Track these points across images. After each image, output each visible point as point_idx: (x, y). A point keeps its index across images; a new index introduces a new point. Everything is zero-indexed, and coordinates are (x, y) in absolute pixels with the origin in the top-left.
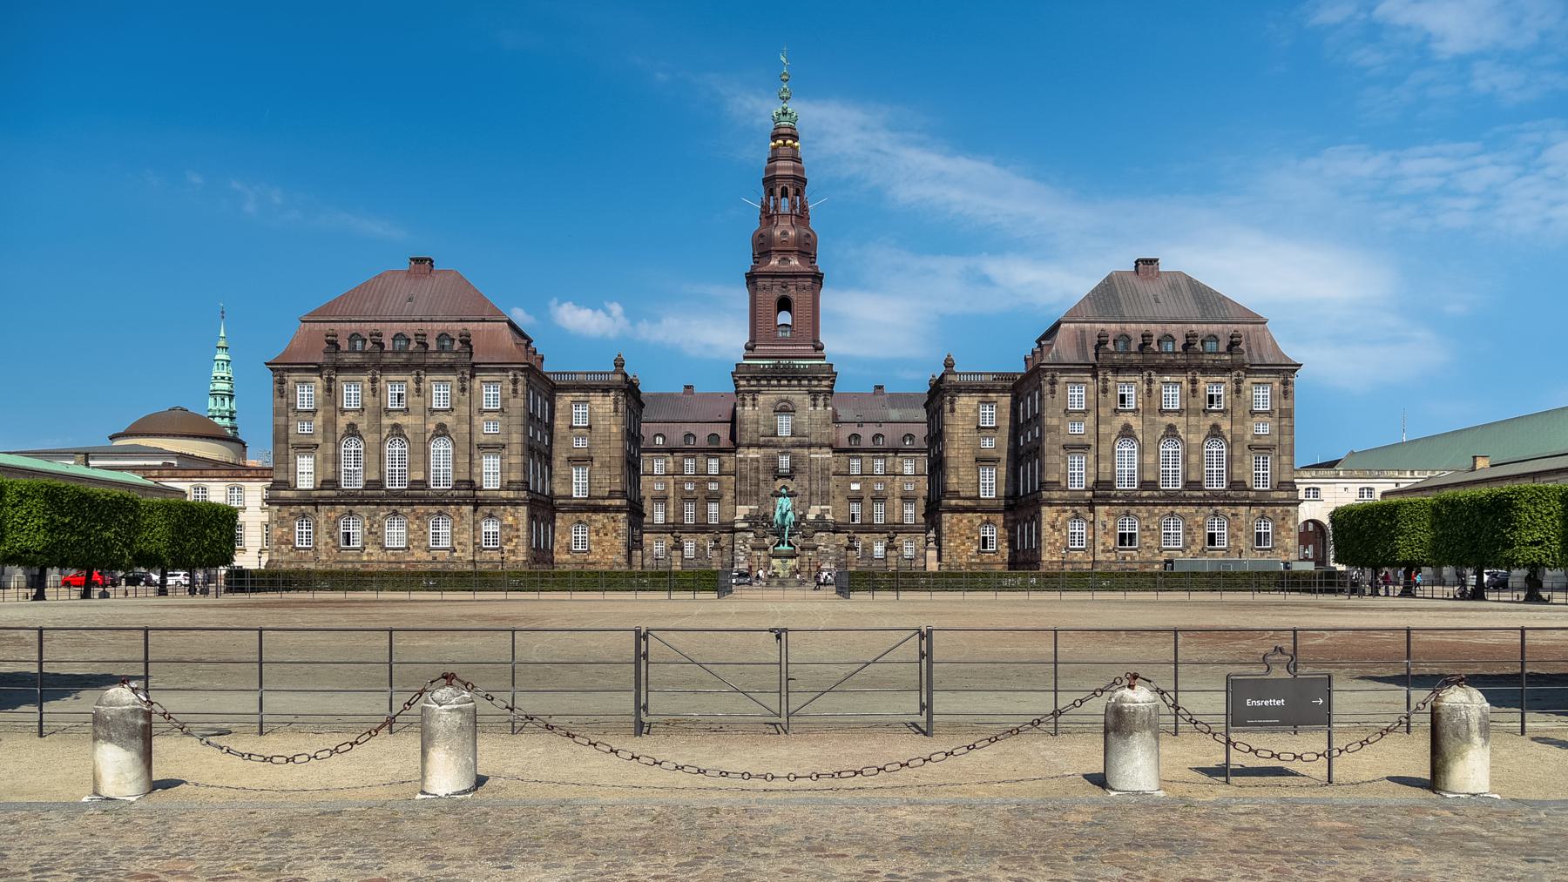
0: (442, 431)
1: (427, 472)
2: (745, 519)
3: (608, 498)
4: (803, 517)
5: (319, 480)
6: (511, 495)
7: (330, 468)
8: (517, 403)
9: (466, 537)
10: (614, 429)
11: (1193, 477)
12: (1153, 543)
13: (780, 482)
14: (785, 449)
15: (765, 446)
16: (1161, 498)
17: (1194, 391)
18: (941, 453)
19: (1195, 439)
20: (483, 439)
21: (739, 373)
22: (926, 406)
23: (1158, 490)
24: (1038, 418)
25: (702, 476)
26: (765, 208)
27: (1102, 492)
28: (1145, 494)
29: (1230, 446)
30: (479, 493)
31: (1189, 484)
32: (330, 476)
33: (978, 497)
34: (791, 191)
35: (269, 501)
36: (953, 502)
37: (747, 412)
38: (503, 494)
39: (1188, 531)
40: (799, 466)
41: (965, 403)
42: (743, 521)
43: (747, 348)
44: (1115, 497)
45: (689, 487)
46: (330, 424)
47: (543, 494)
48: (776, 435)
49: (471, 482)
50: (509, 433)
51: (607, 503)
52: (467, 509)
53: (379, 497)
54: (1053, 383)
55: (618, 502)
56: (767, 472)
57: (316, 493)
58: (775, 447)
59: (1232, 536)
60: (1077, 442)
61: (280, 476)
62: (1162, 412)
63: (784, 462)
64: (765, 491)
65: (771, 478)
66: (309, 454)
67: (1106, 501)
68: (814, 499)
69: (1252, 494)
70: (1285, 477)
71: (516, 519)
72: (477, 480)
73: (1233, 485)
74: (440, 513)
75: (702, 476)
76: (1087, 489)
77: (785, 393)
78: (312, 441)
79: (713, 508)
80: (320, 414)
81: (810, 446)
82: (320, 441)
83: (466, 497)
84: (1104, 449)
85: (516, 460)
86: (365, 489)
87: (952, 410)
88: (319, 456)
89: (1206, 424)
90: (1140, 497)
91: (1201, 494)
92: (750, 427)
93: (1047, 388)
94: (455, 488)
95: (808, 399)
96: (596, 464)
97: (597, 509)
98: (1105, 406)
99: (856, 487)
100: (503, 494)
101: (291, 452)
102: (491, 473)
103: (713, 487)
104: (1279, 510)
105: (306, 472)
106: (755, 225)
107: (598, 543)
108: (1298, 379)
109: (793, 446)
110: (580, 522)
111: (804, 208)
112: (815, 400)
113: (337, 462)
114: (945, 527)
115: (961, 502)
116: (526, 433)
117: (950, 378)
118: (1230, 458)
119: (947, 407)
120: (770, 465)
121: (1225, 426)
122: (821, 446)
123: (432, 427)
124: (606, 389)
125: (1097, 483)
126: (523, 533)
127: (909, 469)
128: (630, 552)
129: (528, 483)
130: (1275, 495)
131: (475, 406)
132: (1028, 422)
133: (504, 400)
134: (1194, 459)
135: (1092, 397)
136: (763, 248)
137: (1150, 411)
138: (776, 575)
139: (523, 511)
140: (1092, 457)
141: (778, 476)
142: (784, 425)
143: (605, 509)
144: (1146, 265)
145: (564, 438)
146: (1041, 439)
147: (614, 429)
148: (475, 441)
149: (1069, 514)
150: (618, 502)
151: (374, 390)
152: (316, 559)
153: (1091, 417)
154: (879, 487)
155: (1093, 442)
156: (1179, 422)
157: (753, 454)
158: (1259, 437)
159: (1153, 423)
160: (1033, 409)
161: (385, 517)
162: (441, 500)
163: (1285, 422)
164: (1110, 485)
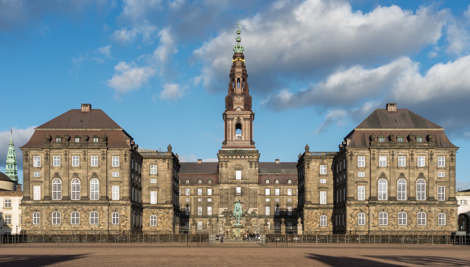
0: (95, 175)
1: (88, 193)
2: (223, 213)
3: (166, 204)
4: (246, 212)
5: (43, 196)
6: (124, 202)
7: (47, 191)
8: (127, 165)
11: (412, 195)
13: (237, 199)
18: (304, 185)
19: (412, 179)
20: (112, 179)
22: (297, 166)
23: (396, 200)
24: (345, 171)
25: (205, 194)
27: (372, 200)
28: (391, 202)
29: (428, 182)
30: (110, 202)
31: (409, 198)
32: (47, 194)
33: (319, 204)
35: (22, 205)
36: (309, 206)
37: (223, 170)
38: (121, 202)
39: (409, 218)
40: (245, 192)
41: (314, 164)
43: (223, 144)
44: (378, 204)
45: (199, 200)
46: (47, 173)
48: (235, 179)
49: (107, 197)
50: (123, 177)
51: (165, 206)
52: (105, 208)
53: (68, 203)
55: (169, 206)
56: (231, 194)
57: (42, 202)
58: (235, 184)
60: (361, 180)
63: (239, 190)
64: (231, 202)
65: (233, 196)
66: (39, 185)
67: (374, 204)
68: (251, 205)
69: (437, 203)
70: (452, 195)
71: (126, 212)
72: (109, 196)
73: (429, 198)
75: (205, 194)
76: (366, 200)
77: (239, 162)
78: (40, 180)
79: (209, 209)
81: (249, 183)
82: (43, 180)
84: (373, 184)
85: (127, 188)
86: (63, 200)
87: (308, 168)
88: (43, 187)
89: (417, 173)
90: (389, 204)
91: (415, 202)
92: (224, 176)
93: (349, 158)
94: (100, 200)
95: (248, 164)
96: (160, 190)
97: (160, 208)
98: (374, 165)
99: (268, 200)
100: (121, 202)
101: (30, 185)
102: (116, 193)
103: (210, 200)
104: (449, 208)
105: (37, 193)
109: (242, 183)
110: (153, 214)
112: (251, 164)
113: (50, 188)
114: (305, 216)
115: (312, 206)
117: (307, 154)
118: (428, 187)
119: (306, 166)
120: (233, 191)
122: (254, 183)
123: (90, 174)
124: (164, 159)
125: (370, 197)
127: (289, 193)
129: (131, 198)
132: (340, 172)
133: (121, 163)
134: (412, 188)
136: (229, 104)
137: (393, 167)
139: (129, 208)
140: (368, 187)
142: (239, 175)
143: (164, 208)
145: (147, 179)
146: (346, 180)
148: (109, 180)
149: (358, 211)
150: (169, 206)
151: (66, 158)
153: (368, 170)
155: (368, 180)
156: (406, 172)
157: (226, 187)
159: (394, 173)
160: (342, 167)
162: (94, 204)
164: (376, 198)
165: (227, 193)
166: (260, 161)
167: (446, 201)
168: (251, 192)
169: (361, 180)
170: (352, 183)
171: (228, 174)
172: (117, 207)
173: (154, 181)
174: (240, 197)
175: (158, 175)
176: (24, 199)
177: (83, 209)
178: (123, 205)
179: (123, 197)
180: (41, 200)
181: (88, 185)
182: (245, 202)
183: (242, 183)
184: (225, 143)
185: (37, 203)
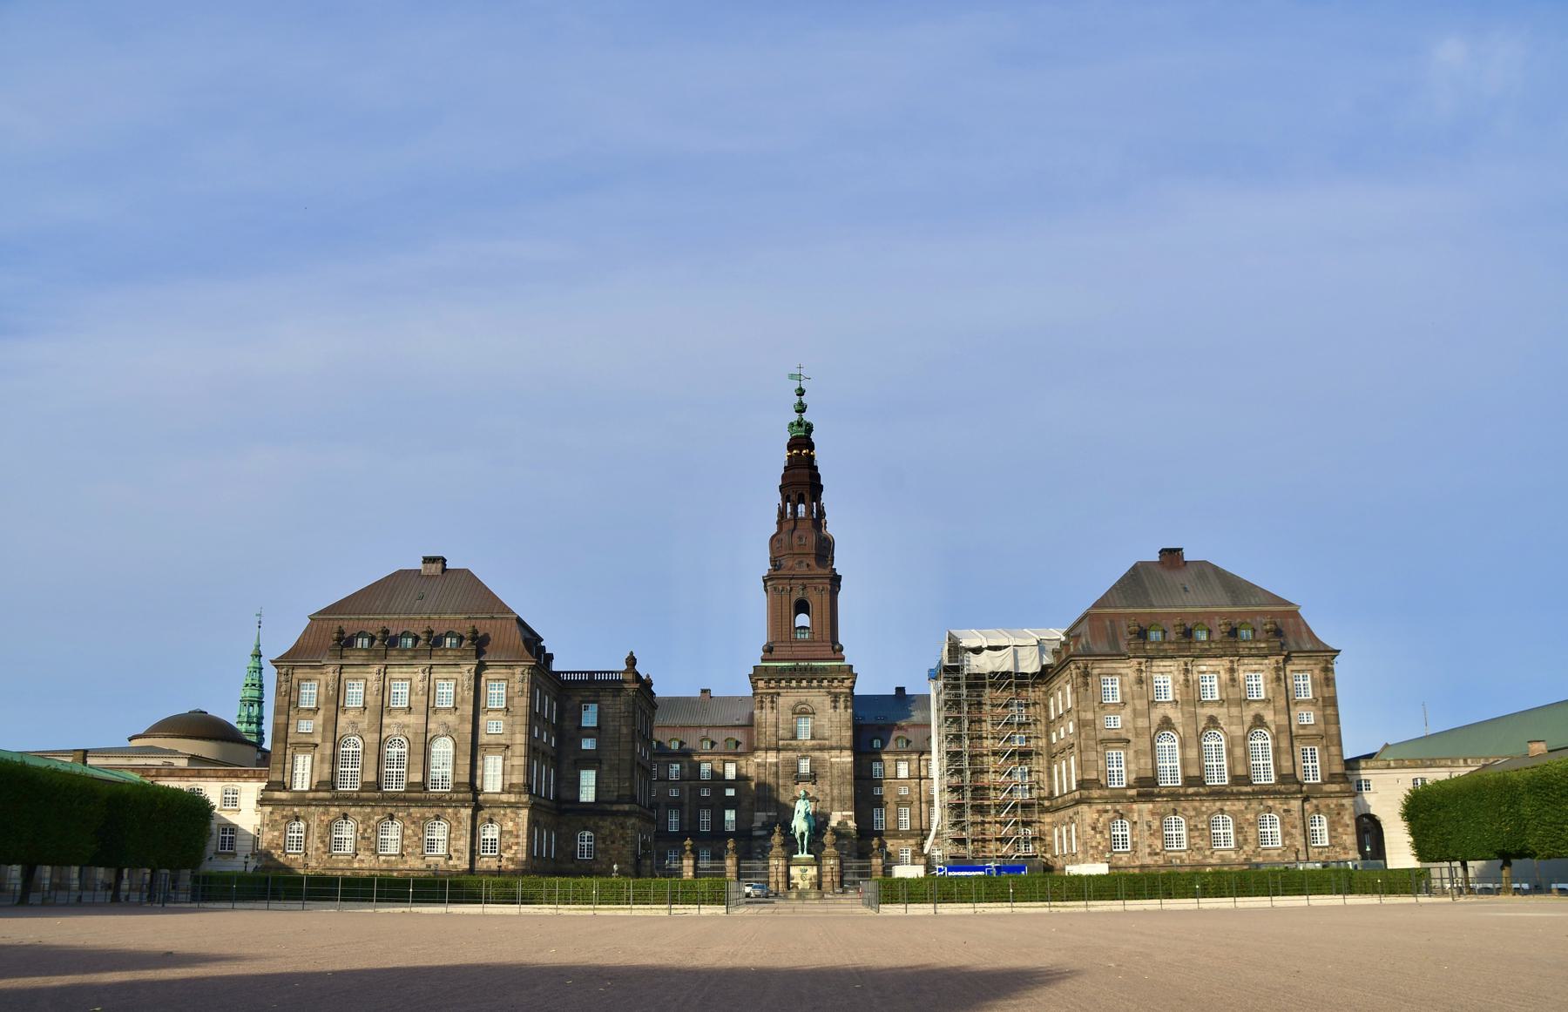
1: (426, 773)
5: (315, 781)
6: (512, 798)
7: (327, 769)
8: (522, 703)
9: (463, 843)
10: (624, 730)
11: (1240, 771)
12: (1202, 844)
14: (805, 752)
15: (785, 749)
16: (1209, 794)
17: (1233, 680)
21: (757, 674)
23: (1203, 784)
26: (782, 513)
27: (1147, 787)
28: (1191, 790)
31: (1236, 780)
34: (807, 497)
35: (262, 802)
37: (766, 716)
38: (504, 798)
40: (819, 771)
42: (760, 829)
44: (1160, 795)
45: (705, 793)
47: (547, 797)
48: (795, 738)
50: (513, 733)
51: (615, 808)
53: (375, 800)
54: (1086, 674)
55: (627, 807)
56: (787, 776)
57: (311, 795)
59: (1286, 834)
61: (276, 777)
62: (1203, 704)
63: (805, 767)
68: (836, 805)
71: (517, 824)
74: (438, 818)
76: (1129, 787)
78: (311, 740)
80: (321, 712)
81: (832, 748)
82: (318, 740)
83: (465, 800)
85: (519, 761)
86: (361, 790)
88: (317, 757)
89: (1248, 717)
91: (1249, 789)
94: (453, 791)
95: (828, 700)
96: (605, 767)
97: (604, 814)
98: (1141, 698)
100: (504, 798)
101: (289, 752)
104: (1333, 803)
105: (304, 772)
106: (775, 530)
107: (605, 851)
108: (1340, 667)
109: (813, 749)
110: (586, 829)
111: (821, 513)
112: (835, 701)
116: (530, 733)
120: (789, 769)
121: (1269, 716)
122: (841, 749)
126: (523, 840)
128: (638, 862)
130: (1328, 788)
131: (482, 704)
134: (1239, 752)
135: (1127, 689)
138: (796, 886)
139: (524, 813)
141: (799, 778)
142: (805, 727)
144: (1171, 556)
147: (624, 730)
150: (627, 807)
152: (306, 866)
154: (904, 791)
156: (1221, 713)
157: (772, 757)
158: (1304, 727)
161: (379, 821)
163: (1329, 711)
165: (777, 773)
166: (857, 692)
167: (1324, 782)
168: (835, 772)
169: (1112, 735)
170: (1092, 743)
171: (777, 726)
172: (495, 810)
173: (588, 744)
174: (809, 785)
175: (598, 727)
176: (271, 787)
177: (409, 815)
178: (510, 805)
179: (511, 785)
180: (311, 790)
181: (427, 753)
182: (820, 797)
183: (813, 749)
184: (769, 649)
185: (301, 800)
